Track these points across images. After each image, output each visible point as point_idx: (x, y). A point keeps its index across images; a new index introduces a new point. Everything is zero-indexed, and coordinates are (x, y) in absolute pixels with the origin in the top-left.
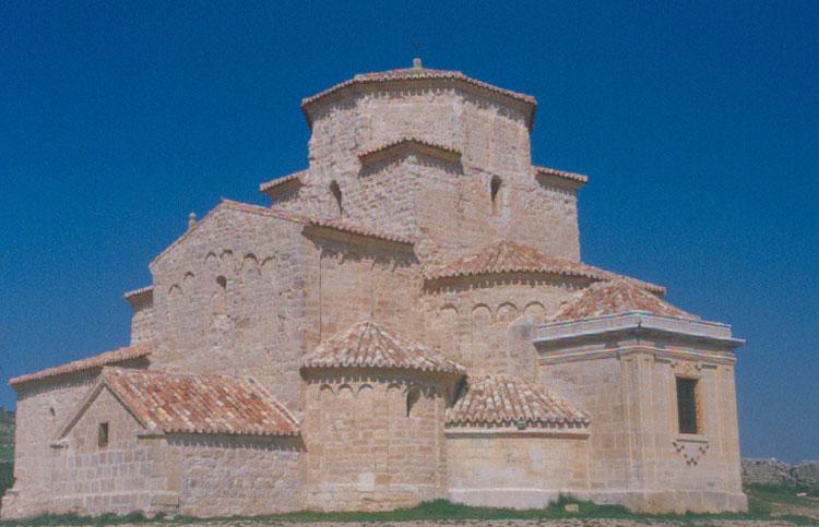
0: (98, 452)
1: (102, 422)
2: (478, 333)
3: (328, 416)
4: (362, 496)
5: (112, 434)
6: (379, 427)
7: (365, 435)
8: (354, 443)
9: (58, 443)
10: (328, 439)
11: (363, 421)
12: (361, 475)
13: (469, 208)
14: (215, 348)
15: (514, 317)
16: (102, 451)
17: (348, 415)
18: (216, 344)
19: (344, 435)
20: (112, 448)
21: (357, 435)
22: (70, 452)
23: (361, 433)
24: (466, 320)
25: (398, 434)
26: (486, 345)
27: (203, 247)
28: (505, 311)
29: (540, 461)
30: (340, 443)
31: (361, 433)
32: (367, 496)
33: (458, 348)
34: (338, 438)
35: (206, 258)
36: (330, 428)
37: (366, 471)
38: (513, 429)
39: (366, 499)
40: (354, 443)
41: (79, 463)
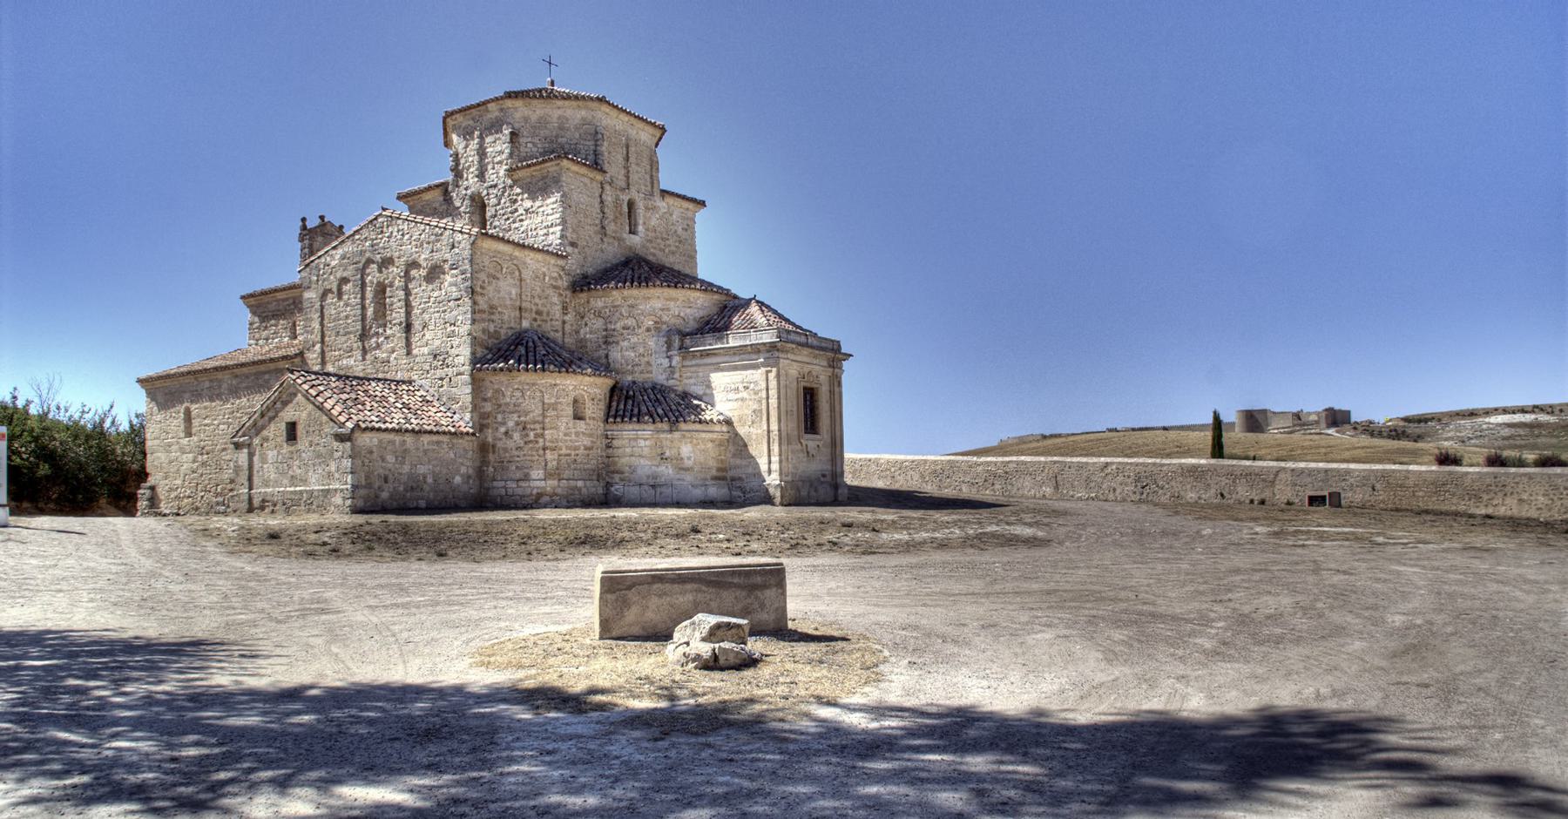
0: (286, 449)
1: (289, 420)
2: (626, 343)
3: (500, 417)
4: (535, 492)
5: (300, 430)
6: (551, 428)
7: (536, 436)
8: (526, 443)
11: (535, 422)
13: (611, 228)
16: (292, 449)
17: (519, 417)
19: (516, 436)
20: (303, 443)
21: (527, 435)
23: (532, 434)
24: (614, 330)
25: (566, 435)
26: (633, 355)
27: (362, 253)
28: (651, 323)
29: (689, 458)
31: (532, 434)
33: (607, 356)
37: (538, 469)
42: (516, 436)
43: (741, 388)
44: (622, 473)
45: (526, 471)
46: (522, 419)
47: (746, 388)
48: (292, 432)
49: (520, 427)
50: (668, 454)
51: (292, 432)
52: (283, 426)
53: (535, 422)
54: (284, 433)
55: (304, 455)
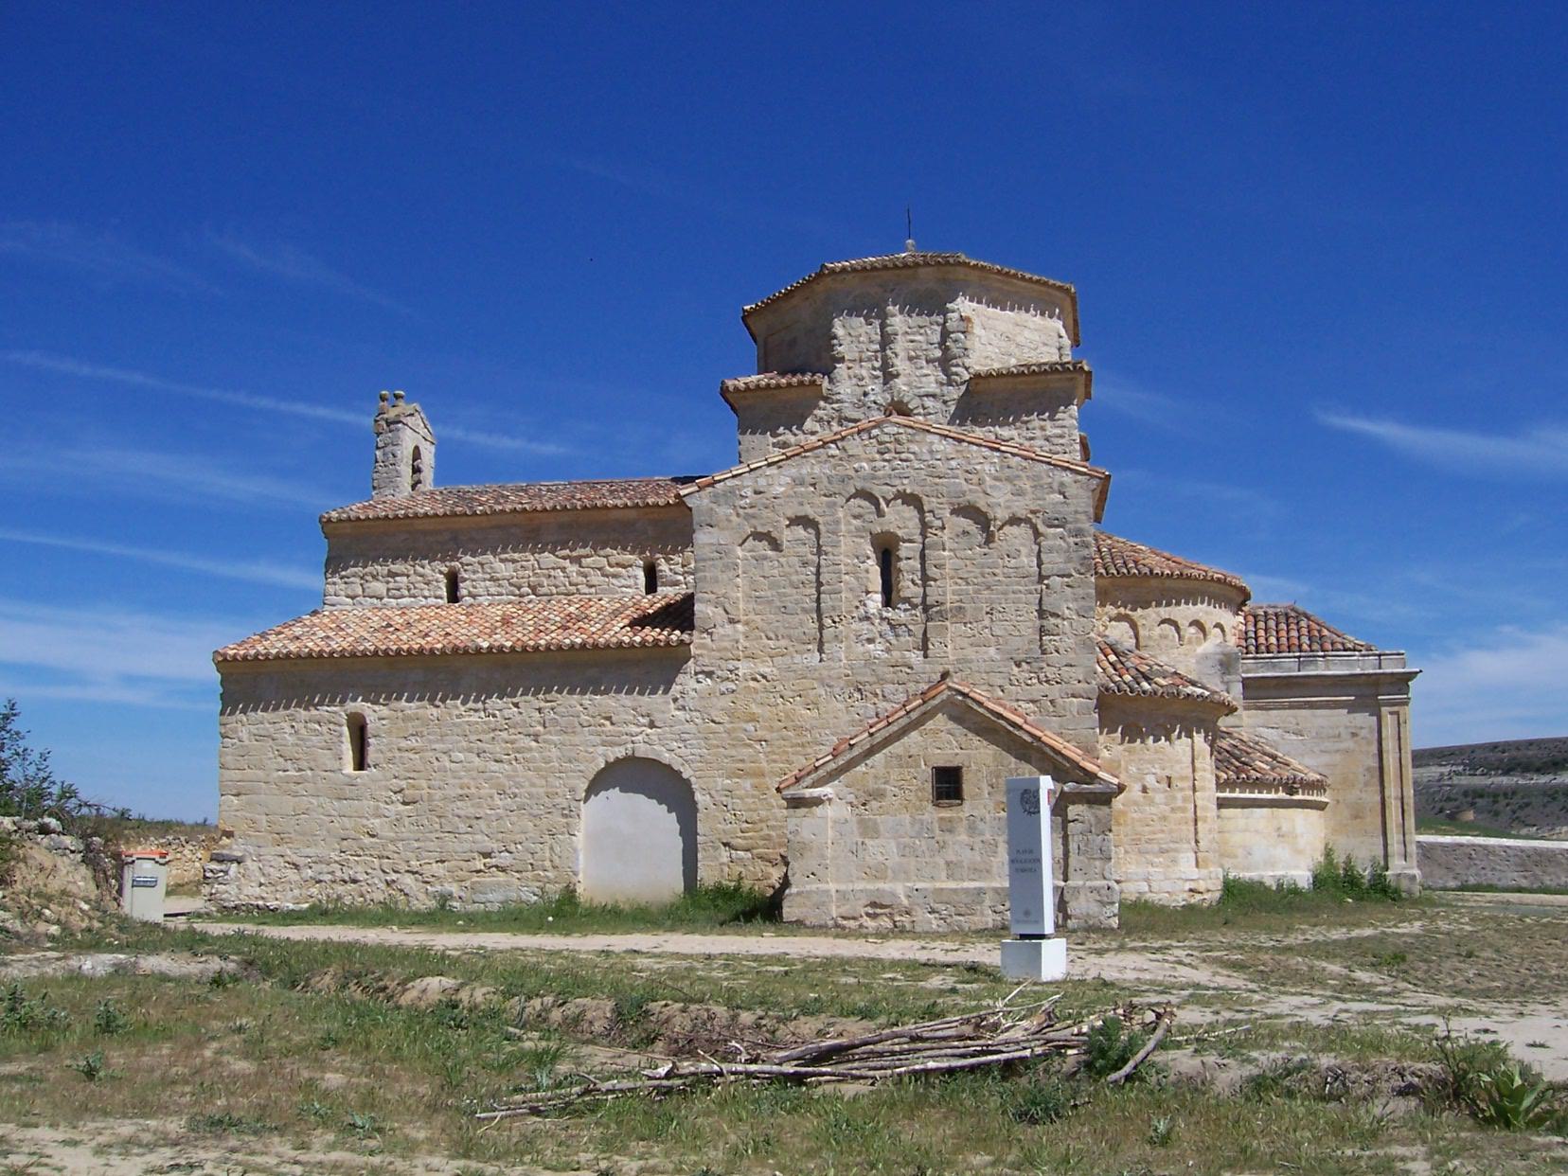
0: (932, 814)
3: (1133, 769)
4: (1188, 886)
7: (1185, 800)
9: (808, 793)
10: (1136, 803)
11: (1182, 778)
12: (1182, 855)
14: (871, 646)
15: (1199, 644)
18: (870, 641)
19: (1159, 798)
21: (1174, 798)
22: (828, 811)
30: (1154, 810)
32: (1193, 885)
34: (1152, 803)
35: (848, 500)
36: (1138, 787)
38: (1282, 795)
39: (1191, 890)
40: (1173, 810)
41: (869, 829)
42: (1159, 798)
43: (1345, 734)
44: (1236, 857)
45: (1172, 854)
46: (1167, 772)
47: (1354, 735)
48: (948, 784)
49: (1165, 785)
50: (1284, 829)
51: (948, 784)
52: (926, 773)
53: (1182, 778)
54: (929, 786)
55: (981, 826)
